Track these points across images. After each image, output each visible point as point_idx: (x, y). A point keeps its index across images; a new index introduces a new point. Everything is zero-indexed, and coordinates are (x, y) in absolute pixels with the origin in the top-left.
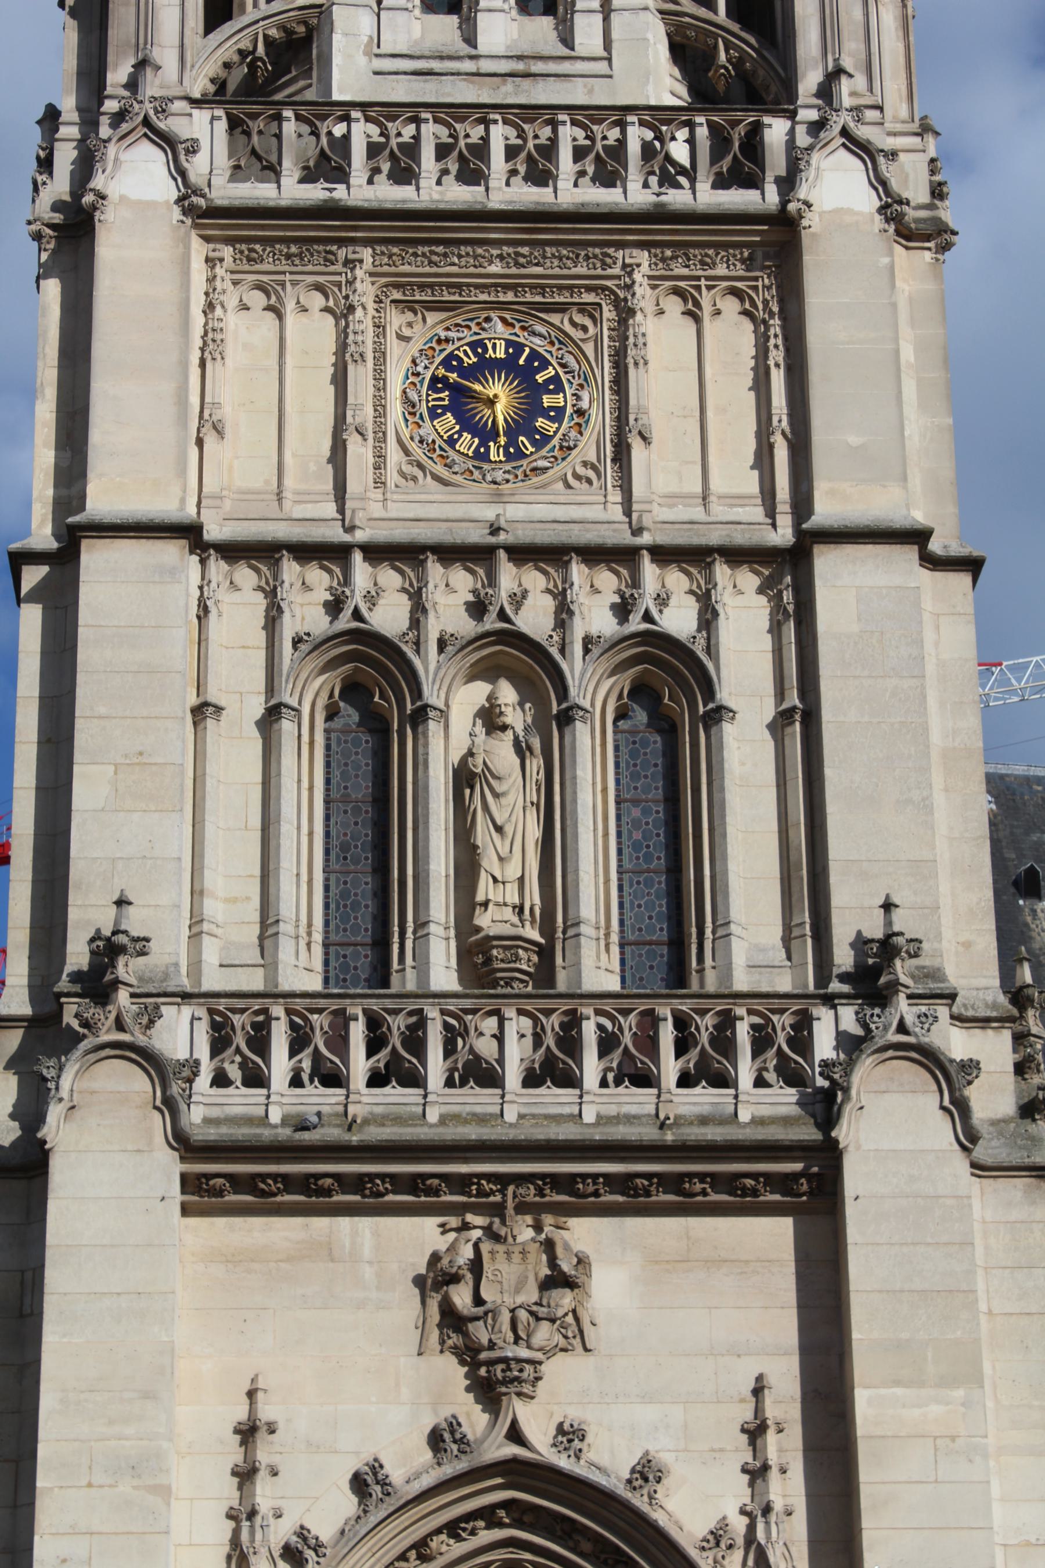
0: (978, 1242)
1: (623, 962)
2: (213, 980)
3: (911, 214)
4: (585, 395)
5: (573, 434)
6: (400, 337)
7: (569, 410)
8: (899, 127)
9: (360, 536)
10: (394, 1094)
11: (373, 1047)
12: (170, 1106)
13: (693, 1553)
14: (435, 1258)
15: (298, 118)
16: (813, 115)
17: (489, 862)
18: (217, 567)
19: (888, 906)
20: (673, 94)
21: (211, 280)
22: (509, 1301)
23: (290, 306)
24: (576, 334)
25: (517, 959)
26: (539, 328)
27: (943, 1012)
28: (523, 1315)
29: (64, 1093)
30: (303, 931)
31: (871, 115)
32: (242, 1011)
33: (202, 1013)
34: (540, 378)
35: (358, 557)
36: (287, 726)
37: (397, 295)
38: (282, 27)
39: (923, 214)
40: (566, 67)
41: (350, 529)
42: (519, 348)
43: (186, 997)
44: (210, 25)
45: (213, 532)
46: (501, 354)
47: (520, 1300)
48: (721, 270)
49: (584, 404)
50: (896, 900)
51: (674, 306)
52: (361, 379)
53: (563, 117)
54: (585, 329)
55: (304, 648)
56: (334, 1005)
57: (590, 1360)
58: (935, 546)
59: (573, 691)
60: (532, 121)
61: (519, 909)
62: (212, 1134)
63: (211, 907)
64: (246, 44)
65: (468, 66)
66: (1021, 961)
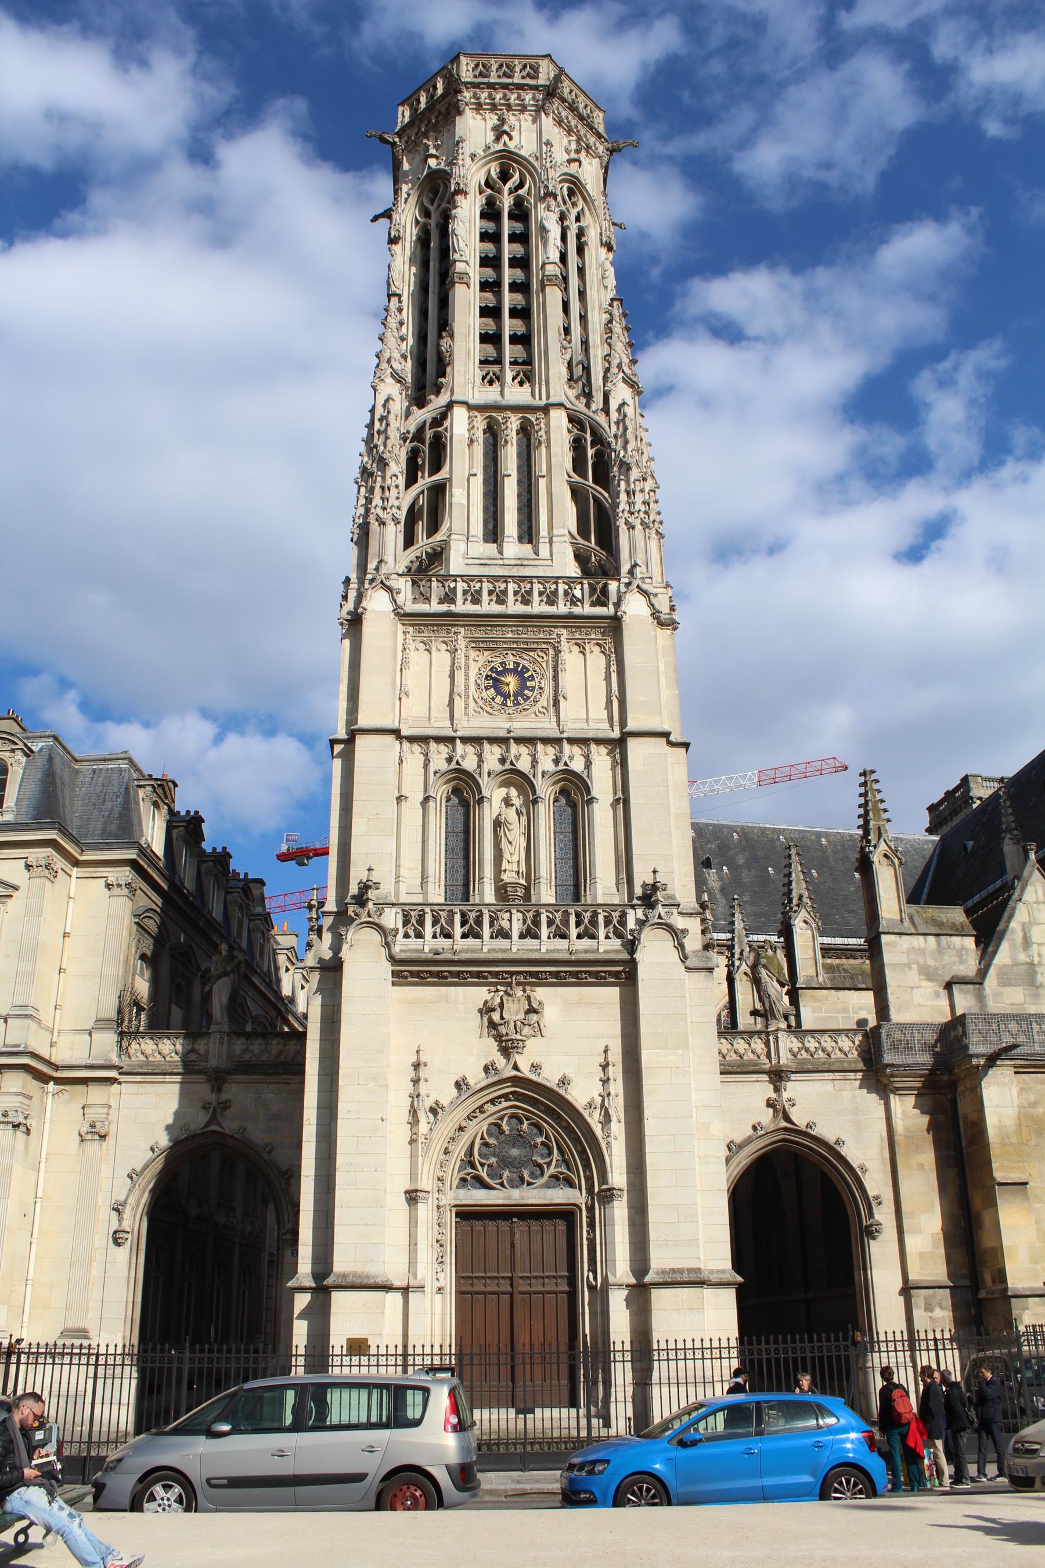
0: (687, 996)
1: (556, 892)
3: (663, 617)
4: (543, 682)
5: (538, 696)
6: (474, 660)
7: (537, 687)
8: (658, 585)
9: (459, 734)
10: (471, 941)
11: (463, 923)
12: (387, 945)
13: (581, 1110)
14: (486, 1002)
15: (437, 580)
16: (627, 580)
17: (506, 855)
18: (406, 745)
19: (655, 872)
21: (405, 639)
23: (434, 649)
24: (540, 660)
25: (517, 891)
26: (526, 657)
27: (675, 911)
28: (519, 1023)
29: (349, 940)
30: (437, 881)
31: (648, 581)
32: (415, 910)
33: (400, 911)
34: (526, 675)
35: (458, 741)
36: (431, 804)
37: (473, 645)
38: (432, 548)
41: (455, 731)
42: (518, 664)
43: (394, 904)
44: (406, 548)
48: (593, 636)
49: (542, 685)
51: (576, 649)
52: (459, 676)
53: (535, 580)
54: (543, 657)
55: (438, 775)
56: (449, 908)
57: (544, 1039)
58: (672, 738)
59: (538, 792)
60: (523, 582)
62: (403, 956)
63: (403, 872)
64: (419, 554)
65: (500, 562)
66: (704, 892)
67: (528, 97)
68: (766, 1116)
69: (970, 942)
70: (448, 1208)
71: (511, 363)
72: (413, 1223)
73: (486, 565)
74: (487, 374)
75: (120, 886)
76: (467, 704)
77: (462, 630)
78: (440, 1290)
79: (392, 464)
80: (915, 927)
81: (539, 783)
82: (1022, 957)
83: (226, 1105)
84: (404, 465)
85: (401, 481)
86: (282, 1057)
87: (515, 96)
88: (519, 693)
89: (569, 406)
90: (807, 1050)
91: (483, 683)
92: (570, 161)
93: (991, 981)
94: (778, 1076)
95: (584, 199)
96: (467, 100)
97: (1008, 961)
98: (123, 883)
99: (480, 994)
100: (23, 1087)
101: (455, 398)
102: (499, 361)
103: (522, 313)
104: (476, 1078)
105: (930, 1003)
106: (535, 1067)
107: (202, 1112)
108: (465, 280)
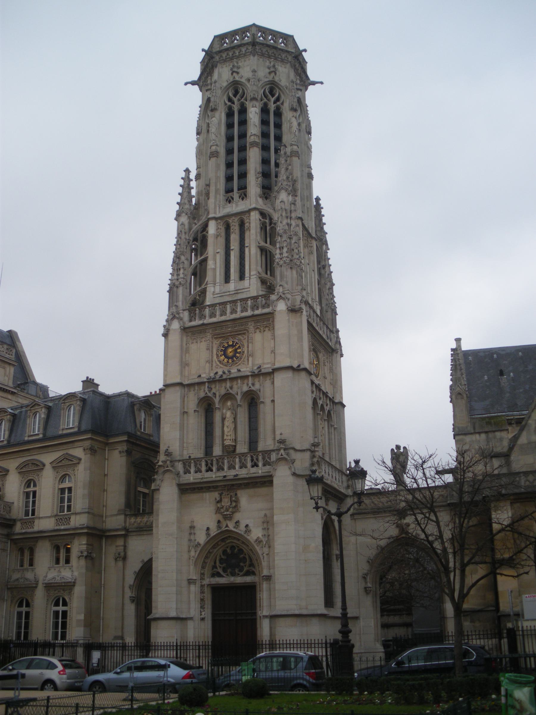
13: (253, 543)
14: (216, 499)
17: (226, 433)
20: (262, 291)
22: (226, 505)
23: (199, 342)
24: (242, 338)
38: (201, 292)
39: (299, 306)
40: (243, 291)
45: (186, 382)
46: (231, 344)
47: (228, 504)
48: (265, 323)
49: (243, 350)
50: (282, 433)
54: (243, 337)
61: (230, 440)
63: (185, 445)
64: (195, 297)
70: (206, 585)
71: (239, 189)
73: (222, 296)
74: (228, 198)
75: (123, 452)
76: (212, 365)
77: (211, 331)
81: (239, 397)
87: (239, 51)
89: (259, 207)
92: (270, 73)
96: (218, 60)
98: (125, 450)
99: (216, 495)
100: (87, 541)
101: (211, 216)
102: (232, 191)
103: (243, 162)
104: (214, 531)
108: (215, 155)
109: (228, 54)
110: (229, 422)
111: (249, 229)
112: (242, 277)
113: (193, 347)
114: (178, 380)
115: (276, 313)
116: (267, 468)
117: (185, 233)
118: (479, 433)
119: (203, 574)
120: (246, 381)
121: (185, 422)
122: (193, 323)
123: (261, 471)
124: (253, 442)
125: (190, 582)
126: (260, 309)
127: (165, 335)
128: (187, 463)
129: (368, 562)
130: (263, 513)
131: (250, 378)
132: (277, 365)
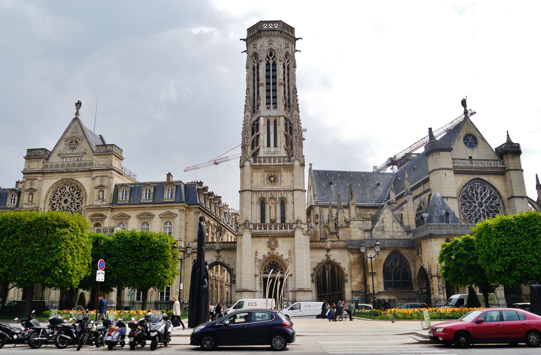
2: (253, 222)
10: (265, 230)
11: (264, 227)
17: (272, 214)
42: (274, 175)
45: (253, 190)
51: (285, 172)
63: (253, 217)
67: (276, 33)
68: (325, 258)
69: (370, 222)
71: (273, 104)
72: (256, 280)
78: (261, 292)
79: (249, 132)
80: (358, 219)
81: (278, 199)
82: (381, 225)
83: (220, 256)
84: (251, 132)
85: (251, 135)
86: (230, 247)
88: (274, 181)
90: (334, 244)
91: (267, 179)
93: (374, 231)
94: (328, 250)
95: (289, 56)
97: (378, 226)
99: (267, 240)
101: (261, 115)
102: (270, 104)
103: (275, 90)
104: (267, 255)
105: (360, 235)
106: (277, 253)
107: (215, 258)
109: (267, 33)
110: (273, 210)
111: (279, 124)
112: (275, 145)
113: (255, 174)
114: (250, 188)
115: (294, 166)
116: (291, 230)
117: (249, 121)
118: (360, 221)
119: (260, 273)
120: (280, 193)
121: (253, 207)
122: (255, 164)
123: (289, 230)
124: (283, 219)
125: (256, 276)
126: (287, 163)
127: (242, 167)
128: (255, 226)
129: (313, 269)
130: (289, 249)
131: (283, 192)
132: (295, 188)
